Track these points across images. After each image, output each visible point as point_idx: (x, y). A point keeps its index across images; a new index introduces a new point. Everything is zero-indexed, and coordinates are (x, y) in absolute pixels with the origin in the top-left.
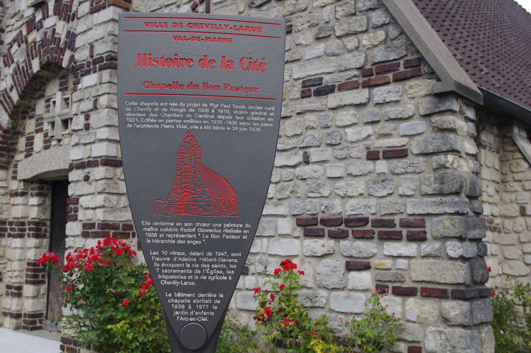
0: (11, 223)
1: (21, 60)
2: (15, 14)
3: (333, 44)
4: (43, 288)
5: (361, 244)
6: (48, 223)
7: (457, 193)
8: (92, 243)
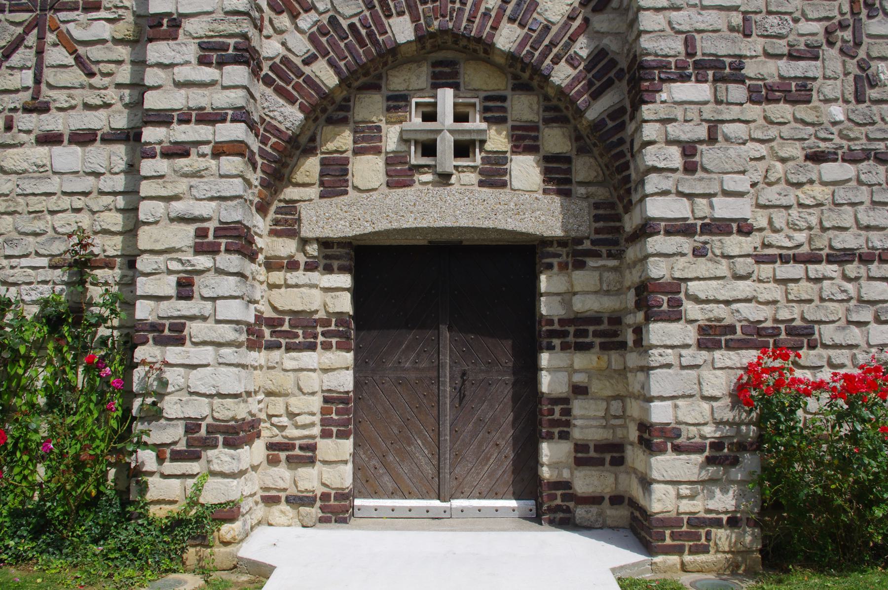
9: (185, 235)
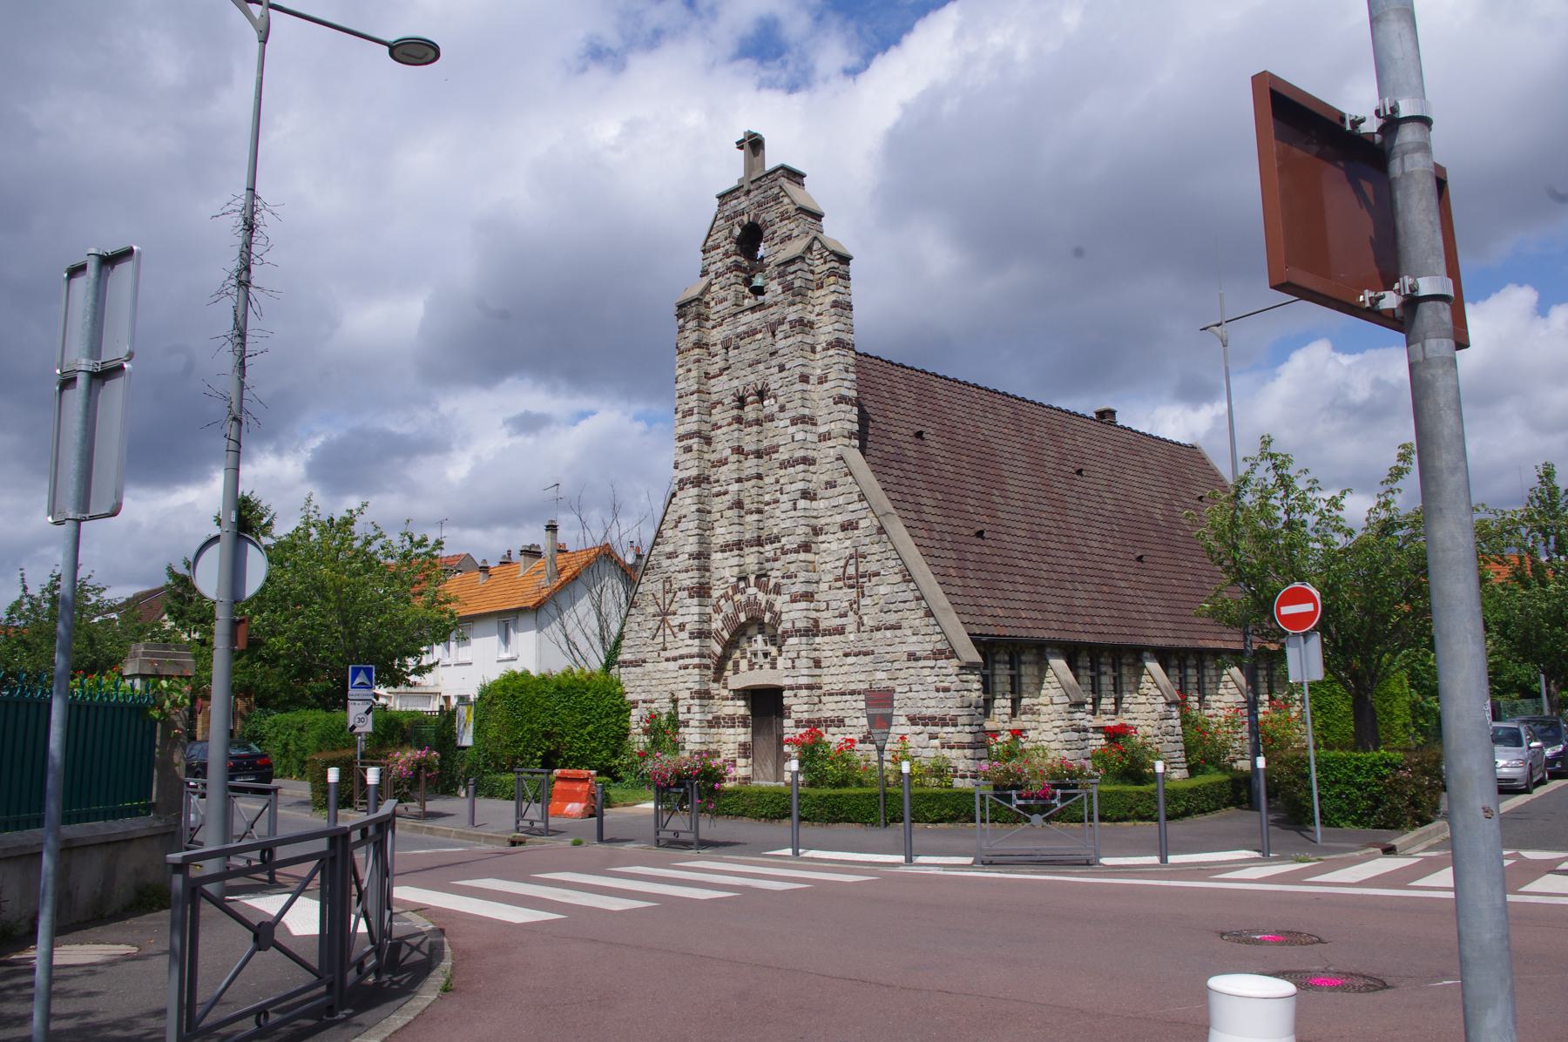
0: (724, 719)
1: (730, 611)
3: (920, 638)
4: (750, 760)
7: (969, 707)
8: (802, 731)
9: (687, 694)
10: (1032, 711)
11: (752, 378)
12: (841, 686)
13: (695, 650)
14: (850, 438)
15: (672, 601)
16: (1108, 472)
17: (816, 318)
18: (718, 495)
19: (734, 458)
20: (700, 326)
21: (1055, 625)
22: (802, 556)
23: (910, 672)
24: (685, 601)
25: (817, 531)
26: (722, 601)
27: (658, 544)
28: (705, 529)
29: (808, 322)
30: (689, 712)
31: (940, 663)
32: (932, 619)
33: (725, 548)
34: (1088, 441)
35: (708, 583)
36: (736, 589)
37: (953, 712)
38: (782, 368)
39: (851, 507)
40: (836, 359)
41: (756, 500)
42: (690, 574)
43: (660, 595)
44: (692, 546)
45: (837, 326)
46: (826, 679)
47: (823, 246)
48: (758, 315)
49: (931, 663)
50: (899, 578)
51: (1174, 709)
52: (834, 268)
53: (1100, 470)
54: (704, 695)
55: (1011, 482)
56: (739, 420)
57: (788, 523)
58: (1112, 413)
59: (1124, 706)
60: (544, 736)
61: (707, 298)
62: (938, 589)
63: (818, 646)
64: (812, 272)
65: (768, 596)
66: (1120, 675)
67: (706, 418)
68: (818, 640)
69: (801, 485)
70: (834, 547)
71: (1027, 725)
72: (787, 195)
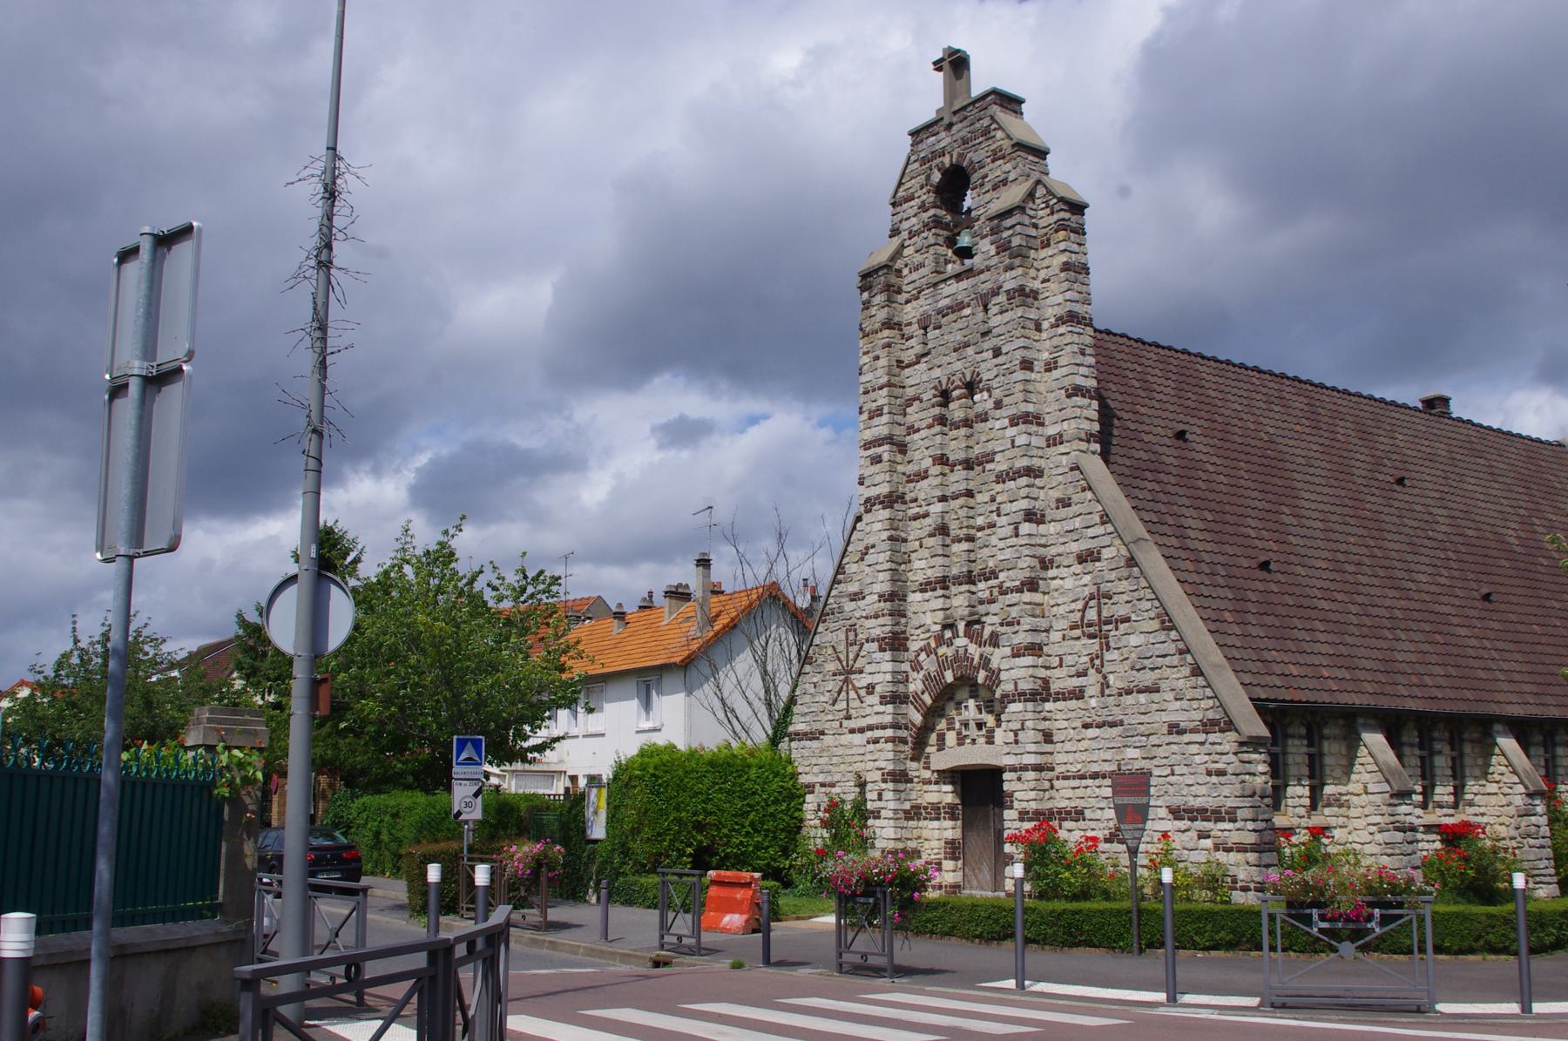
0: (926, 808)
2: (920, 626)
3: (1185, 704)
4: (960, 863)
5: (1205, 823)
6: (960, 807)
7: (1252, 796)
8: (1029, 825)
9: (877, 776)
10: (1338, 802)
11: (958, 365)
12: (1079, 766)
13: (888, 719)
14: (1088, 441)
15: (858, 655)
16: (1441, 481)
17: (1041, 286)
18: (916, 518)
19: (937, 469)
20: (890, 301)
21: (1369, 688)
22: (1027, 596)
23: (1172, 749)
24: (874, 655)
25: (1045, 564)
26: (923, 656)
27: (840, 582)
28: (899, 562)
29: (1032, 291)
30: (880, 799)
31: (1212, 737)
32: (1200, 678)
33: (926, 587)
34: (1412, 439)
35: (904, 632)
36: (940, 640)
37: (1230, 803)
38: (997, 352)
39: (1091, 532)
40: (1068, 338)
41: (965, 524)
42: (881, 621)
43: (841, 648)
44: (882, 585)
45: (1069, 295)
46: (1060, 758)
47: (1049, 192)
48: (964, 284)
49: (1200, 737)
50: (1155, 625)
51: (1537, 802)
52: (1063, 220)
53: (1428, 478)
54: (899, 777)
55: (1306, 495)
56: (942, 420)
57: (1008, 554)
58: (1445, 401)
59: (1467, 797)
60: (694, 828)
61: (899, 264)
62: (1209, 638)
63: (1048, 715)
64: (1035, 226)
65: (983, 649)
66: (1461, 755)
67: (899, 418)
68: (1048, 706)
69: (1024, 504)
70: (1068, 584)
71: (1332, 821)
72: (1000, 128)
